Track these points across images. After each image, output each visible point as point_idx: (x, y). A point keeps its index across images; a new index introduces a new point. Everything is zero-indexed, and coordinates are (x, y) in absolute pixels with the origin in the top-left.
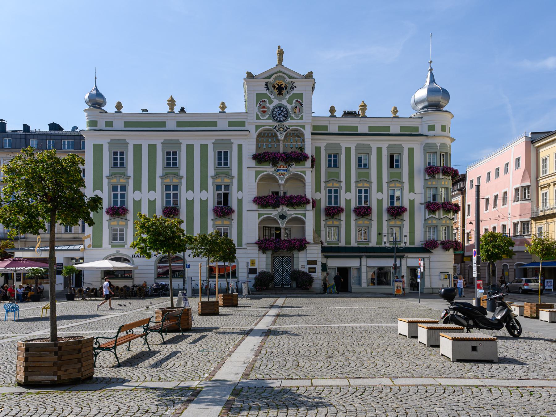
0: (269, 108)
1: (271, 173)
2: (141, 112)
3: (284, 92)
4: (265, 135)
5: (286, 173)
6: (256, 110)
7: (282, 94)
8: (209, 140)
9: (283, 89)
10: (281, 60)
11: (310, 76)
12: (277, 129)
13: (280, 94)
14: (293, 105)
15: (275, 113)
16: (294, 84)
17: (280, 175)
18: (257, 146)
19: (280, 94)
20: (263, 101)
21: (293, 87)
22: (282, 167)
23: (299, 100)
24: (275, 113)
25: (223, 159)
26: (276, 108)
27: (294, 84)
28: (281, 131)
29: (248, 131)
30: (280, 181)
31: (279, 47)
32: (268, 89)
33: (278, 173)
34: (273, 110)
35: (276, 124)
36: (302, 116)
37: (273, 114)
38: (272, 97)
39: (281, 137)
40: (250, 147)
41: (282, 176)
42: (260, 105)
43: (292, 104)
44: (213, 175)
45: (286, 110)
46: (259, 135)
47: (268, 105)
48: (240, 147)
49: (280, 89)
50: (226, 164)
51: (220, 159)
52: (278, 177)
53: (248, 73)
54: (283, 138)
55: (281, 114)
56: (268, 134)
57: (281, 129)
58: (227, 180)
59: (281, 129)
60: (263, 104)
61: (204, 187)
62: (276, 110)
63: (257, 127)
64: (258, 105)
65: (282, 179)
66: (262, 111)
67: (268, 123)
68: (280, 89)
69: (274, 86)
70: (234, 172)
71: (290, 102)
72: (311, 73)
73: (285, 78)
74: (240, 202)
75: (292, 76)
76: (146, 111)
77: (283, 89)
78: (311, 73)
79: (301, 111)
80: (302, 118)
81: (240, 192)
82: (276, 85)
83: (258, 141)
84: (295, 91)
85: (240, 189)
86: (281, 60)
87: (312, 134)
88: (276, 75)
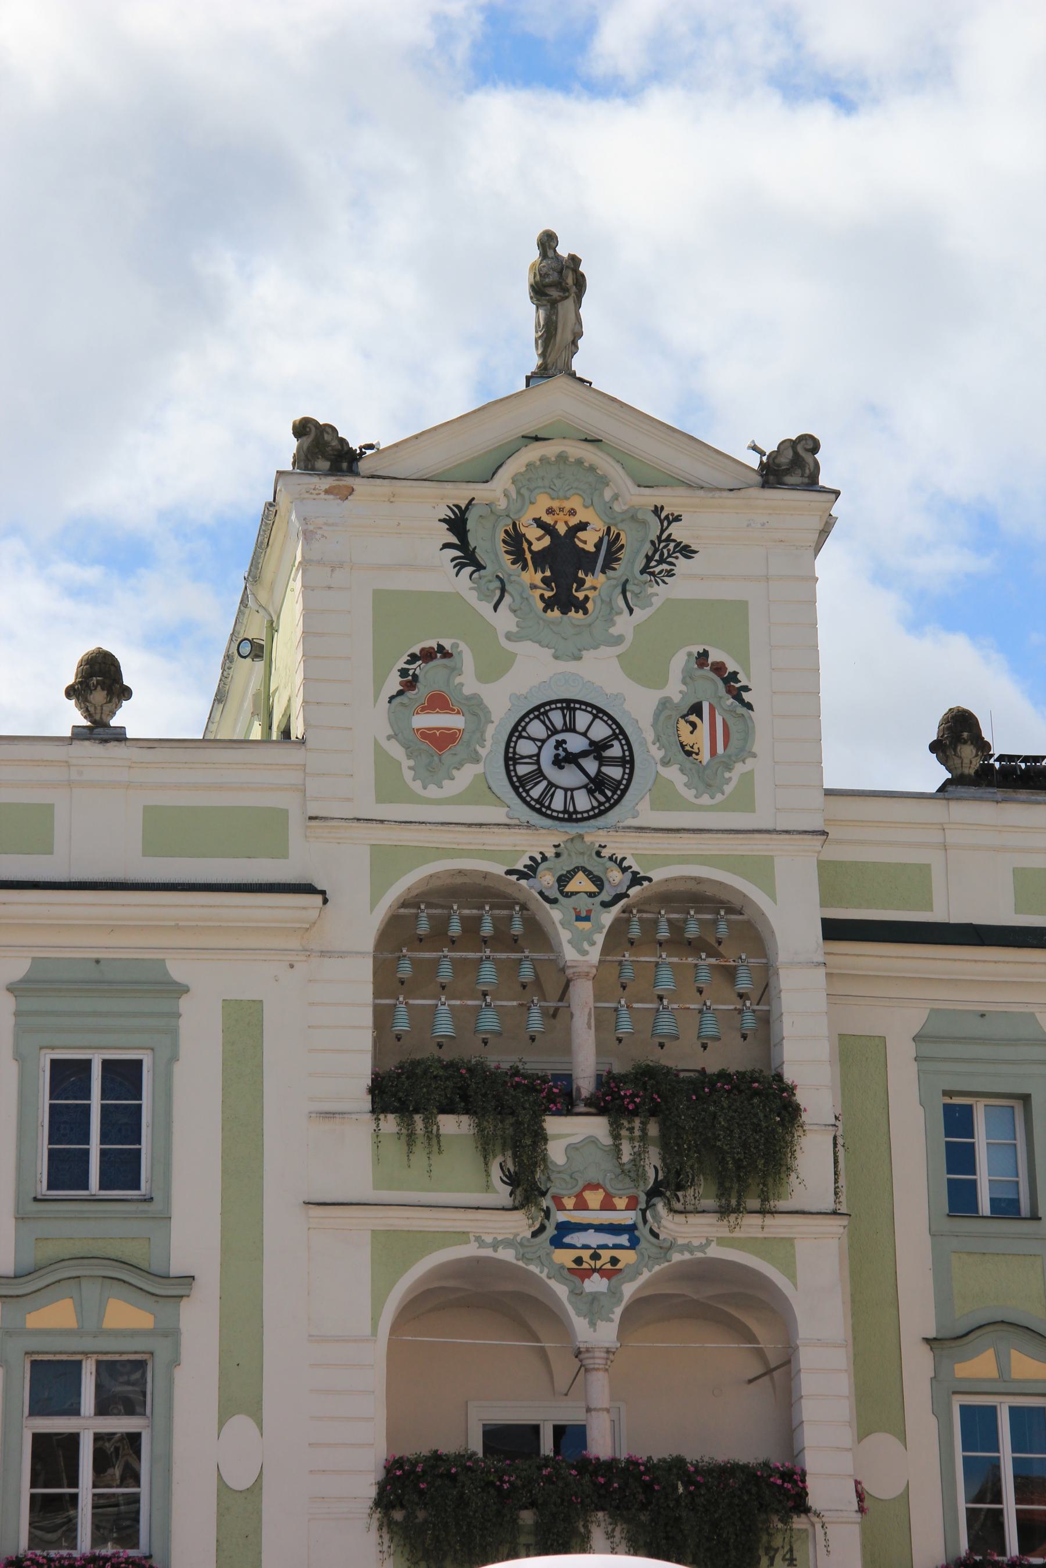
0: (476, 709)
1: (507, 1255)
3: (596, 584)
4: (446, 930)
5: (627, 1257)
6: (372, 719)
7: (581, 606)
9: (587, 561)
10: (557, 340)
11: (792, 466)
12: (547, 879)
13: (564, 599)
14: (675, 690)
15: (525, 748)
16: (676, 531)
17: (579, 1272)
18: (382, 1018)
20: (427, 655)
21: (666, 553)
22: (594, 1198)
23: (715, 656)
24: (525, 748)
26: (539, 712)
27: (676, 531)
28: (584, 903)
29: (308, 889)
30: (580, 1324)
31: (548, 241)
32: (468, 557)
33: (564, 1257)
34: (517, 731)
35: (543, 839)
36: (748, 778)
37: (511, 759)
38: (504, 620)
39: (579, 945)
40: (327, 1027)
41: (596, 1284)
42: (410, 682)
45: (619, 733)
46: (397, 934)
48: (244, 1024)
49: (565, 568)
50: (123, 1171)
51: (67, 1124)
52: (561, 1291)
53: (303, 428)
54: (594, 955)
55: (576, 763)
56: (471, 926)
57: (581, 883)
58: (125, 1317)
59: (581, 883)
60: (430, 674)
62: (536, 728)
63: (385, 862)
64: (393, 683)
66: (427, 735)
67: (478, 832)
68: (565, 568)
69: (515, 541)
70: (192, 1232)
71: (643, 669)
72: (809, 444)
73: (604, 481)
75: (674, 461)
77: (587, 561)
78: (809, 444)
79: (736, 744)
80: (745, 800)
81: (241, 1423)
82: (532, 533)
83: (387, 982)
84: (685, 582)
85: (241, 1394)
86: (557, 340)
87: (834, 930)
88: (533, 453)
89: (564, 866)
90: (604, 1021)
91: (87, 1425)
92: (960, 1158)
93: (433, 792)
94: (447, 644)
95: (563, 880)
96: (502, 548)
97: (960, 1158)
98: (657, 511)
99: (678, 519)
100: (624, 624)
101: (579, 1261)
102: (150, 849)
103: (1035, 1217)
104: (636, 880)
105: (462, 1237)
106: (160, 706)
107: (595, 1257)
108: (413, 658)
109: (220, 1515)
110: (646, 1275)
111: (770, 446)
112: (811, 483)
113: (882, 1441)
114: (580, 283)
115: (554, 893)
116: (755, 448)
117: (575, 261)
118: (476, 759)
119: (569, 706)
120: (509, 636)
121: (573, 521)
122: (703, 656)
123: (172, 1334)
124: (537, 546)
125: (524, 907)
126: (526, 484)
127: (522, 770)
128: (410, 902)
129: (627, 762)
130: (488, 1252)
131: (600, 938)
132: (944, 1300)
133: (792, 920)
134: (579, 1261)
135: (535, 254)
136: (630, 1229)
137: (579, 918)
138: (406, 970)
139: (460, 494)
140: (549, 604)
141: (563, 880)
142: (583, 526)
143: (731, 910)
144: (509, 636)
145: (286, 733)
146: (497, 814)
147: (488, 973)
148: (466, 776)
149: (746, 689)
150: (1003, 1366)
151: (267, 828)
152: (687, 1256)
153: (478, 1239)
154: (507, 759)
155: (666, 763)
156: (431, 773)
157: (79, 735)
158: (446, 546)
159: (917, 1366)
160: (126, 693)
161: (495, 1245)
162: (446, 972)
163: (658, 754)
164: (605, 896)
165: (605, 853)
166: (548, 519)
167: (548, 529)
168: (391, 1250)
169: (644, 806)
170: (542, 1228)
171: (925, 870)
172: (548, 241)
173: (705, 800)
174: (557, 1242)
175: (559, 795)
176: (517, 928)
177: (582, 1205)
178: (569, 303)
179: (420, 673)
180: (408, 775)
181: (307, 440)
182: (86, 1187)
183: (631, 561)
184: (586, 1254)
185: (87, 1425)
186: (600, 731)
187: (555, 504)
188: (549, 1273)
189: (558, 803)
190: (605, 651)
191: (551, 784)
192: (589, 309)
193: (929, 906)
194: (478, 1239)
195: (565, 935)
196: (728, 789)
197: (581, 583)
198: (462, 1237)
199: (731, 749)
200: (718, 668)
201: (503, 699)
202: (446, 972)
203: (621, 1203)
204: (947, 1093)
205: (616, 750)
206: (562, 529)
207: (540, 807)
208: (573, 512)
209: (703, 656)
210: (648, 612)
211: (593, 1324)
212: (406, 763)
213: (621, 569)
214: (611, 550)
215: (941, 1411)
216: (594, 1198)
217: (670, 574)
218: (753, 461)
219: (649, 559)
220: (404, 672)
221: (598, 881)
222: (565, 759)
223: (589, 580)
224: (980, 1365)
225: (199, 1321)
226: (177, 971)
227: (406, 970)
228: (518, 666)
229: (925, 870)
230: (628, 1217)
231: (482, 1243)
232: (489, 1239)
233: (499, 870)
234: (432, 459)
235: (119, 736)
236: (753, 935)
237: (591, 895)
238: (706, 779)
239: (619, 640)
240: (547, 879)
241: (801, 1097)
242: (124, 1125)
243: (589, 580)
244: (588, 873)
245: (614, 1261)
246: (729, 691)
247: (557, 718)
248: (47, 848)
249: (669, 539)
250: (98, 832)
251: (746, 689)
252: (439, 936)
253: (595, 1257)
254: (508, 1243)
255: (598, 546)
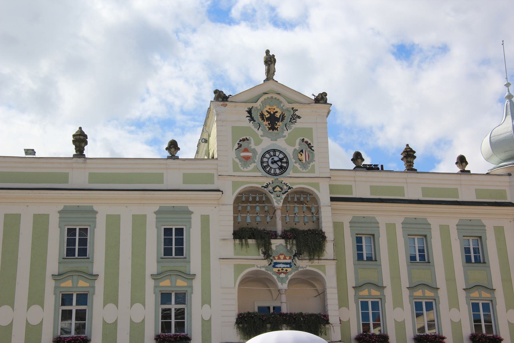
0: (254, 151)
1: (263, 269)
2: (23, 155)
3: (280, 124)
4: (248, 200)
5: (289, 270)
6: (232, 154)
7: (277, 129)
8: (149, 207)
9: (278, 119)
10: (270, 73)
11: (321, 99)
12: (270, 188)
13: (273, 128)
14: (297, 147)
15: (265, 160)
16: (296, 113)
17: (279, 273)
18: (235, 218)
19: (273, 128)
20: (244, 140)
21: (295, 118)
23: (306, 140)
24: (265, 160)
25: (174, 242)
26: (268, 152)
27: (296, 113)
28: (278, 193)
29: (219, 191)
30: (279, 284)
31: (268, 52)
32: (252, 119)
33: (276, 270)
34: (263, 156)
35: (269, 180)
36: (313, 166)
37: (262, 162)
38: (260, 132)
39: (278, 203)
40: (223, 222)
41: (283, 275)
42: (240, 146)
43: (294, 146)
44: (155, 272)
45: (285, 156)
46: (238, 200)
47: (253, 146)
49: (273, 121)
50: (180, 252)
51: (168, 242)
52: (275, 277)
53: (216, 92)
56: (254, 198)
57: (278, 189)
58: (181, 283)
59: (278, 189)
60: (244, 144)
61: (137, 297)
63: (235, 185)
64: (236, 146)
65: (282, 281)
67: (256, 178)
68: (273, 121)
69: (262, 115)
70: (195, 265)
71: (291, 143)
73: (281, 102)
74: (206, 325)
75: (296, 98)
76: (33, 152)
77: (278, 119)
79: (311, 158)
80: (313, 170)
81: (206, 306)
82: (266, 114)
83: (236, 211)
84: (299, 124)
85: (206, 300)
86: (270, 73)
87: (333, 199)
88: (265, 96)
89: (274, 185)
90: (283, 219)
91: (173, 306)
92: (360, 248)
93: (245, 169)
94: (248, 138)
95: (274, 188)
96: (259, 117)
97: (360, 248)
98: (293, 109)
99: (297, 110)
100: (286, 133)
101: (279, 270)
102: (184, 182)
103: (376, 260)
104: (290, 188)
105: (253, 266)
106: (188, 150)
107: (282, 270)
108: (241, 141)
109: (202, 326)
110: (293, 273)
111: (317, 95)
112: (325, 102)
113: (344, 309)
114: (275, 60)
115: (272, 191)
116: (313, 95)
117: (273, 56)
118: (254, 162)
119: (274, 151)
120: (261, 136)
121: (274, 111)
122: (303, 139)
123: (191, 287)
124: (267, 116)
125: (265, 194)
126: (264, 103)
127: (265, 165)
128: (240, 194)
129: (287, 163)
130: (259, 269)
131: (282, 201)
132: (357, 278)
133: (324, 197)
134: (279, 270)
135: (265, 55)
136: (290, 264)
137: (277, 196)
138: (240, 208)
139: (250, 105)
140: (270, 129)
141: (274, 188)
142: (277, 112)
143: (310, 195)
144: (261, 136)
145: (213, 158)
146: (260, 174)
147: (258, 209)
148: (253, 166)
149: (312, 147)
150: (369, 292)
151: (210, 178)
152: (302, 269)
153: (257, 266)
154: (261, 162)
155: (296, 163)
156: (245, 165)
157: (169, 158)
158: (247, 117)
159: (351, 293)
160: (179, 149)
161: (261, 267)
162: (249, 208)
163: (294, 161)
164: (283, 192)
165: (283, 182)
166: (269, 111)
167: (269, 113)
168: (238, 268)
169: (291, 172)
170: (271, 264)
171: (351, 186)
172: (268, 52)
173: (304, 171)
174: (274, 267)
175: (273, 170)
176: (264, 199)
177: (279, 258)
178: (273, 65)
179: (242, 144)
180: (240, 166)
181: (217, 94)
182: (172, 255)
183: (287, 119)
184: (280, 269)
185: (173, 306)
186: (281, 156)
187: (271, 107)
188: (272, 273)
189: (272, 172)
190: (282, 139)
191: (271, 168)
192: (277, 66)
193: (352, 194)
194: (257, 266)
195: (274, 200)
196: (309, 168)
197: (276, 124)
198: (253, 266)
199: (310, 160)
200: (306, 142)
201: (260, 150)
202: (249, 208)
203: (288, 258)
204: (357, 234)
205: (285, 160)
206: (272, 113)
207: (269, 173)
208: (274, 109)
209: (303, 139)
210: (291, 130)
211: (282, 284)
212: (239, 163)
213: (285, 121)
214: (283, 117)
215: (356, 302)
216: (282, 257)
217: (296, 122)
218: (313, 98)
219: (291, 119)
220: (238, 144)
221: (281, 189)
222: (274, 162)
223: (278, 124)
224: (365, 292)
225: (197, 284)
226: (191, 209)
227: (240, 208)
228: (263, 142)
229: (351, 186)
230: (289, 261)
231: (257, 267)
232: (259, 266)
233: (260, 186)
234: (244, 98)
235: (177, 158)
236: (315, 200)
237: (280, 191)
238: (304, 166)
239: (285, 136)
240: (270, 188)
241: (326, 235)
242: (180, 242)
243: (278, 124)
244: (279, 187)
245: (286, 270)
246: (309, 147)
247: (272, 153)
248: (162, 182)
249: (295, 115)
250: (173, 178)
251: (312, 147)
252: (247, 201)
253: (282, 270)
254: (263, 267)
255: (280, 116)
